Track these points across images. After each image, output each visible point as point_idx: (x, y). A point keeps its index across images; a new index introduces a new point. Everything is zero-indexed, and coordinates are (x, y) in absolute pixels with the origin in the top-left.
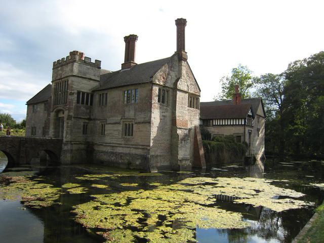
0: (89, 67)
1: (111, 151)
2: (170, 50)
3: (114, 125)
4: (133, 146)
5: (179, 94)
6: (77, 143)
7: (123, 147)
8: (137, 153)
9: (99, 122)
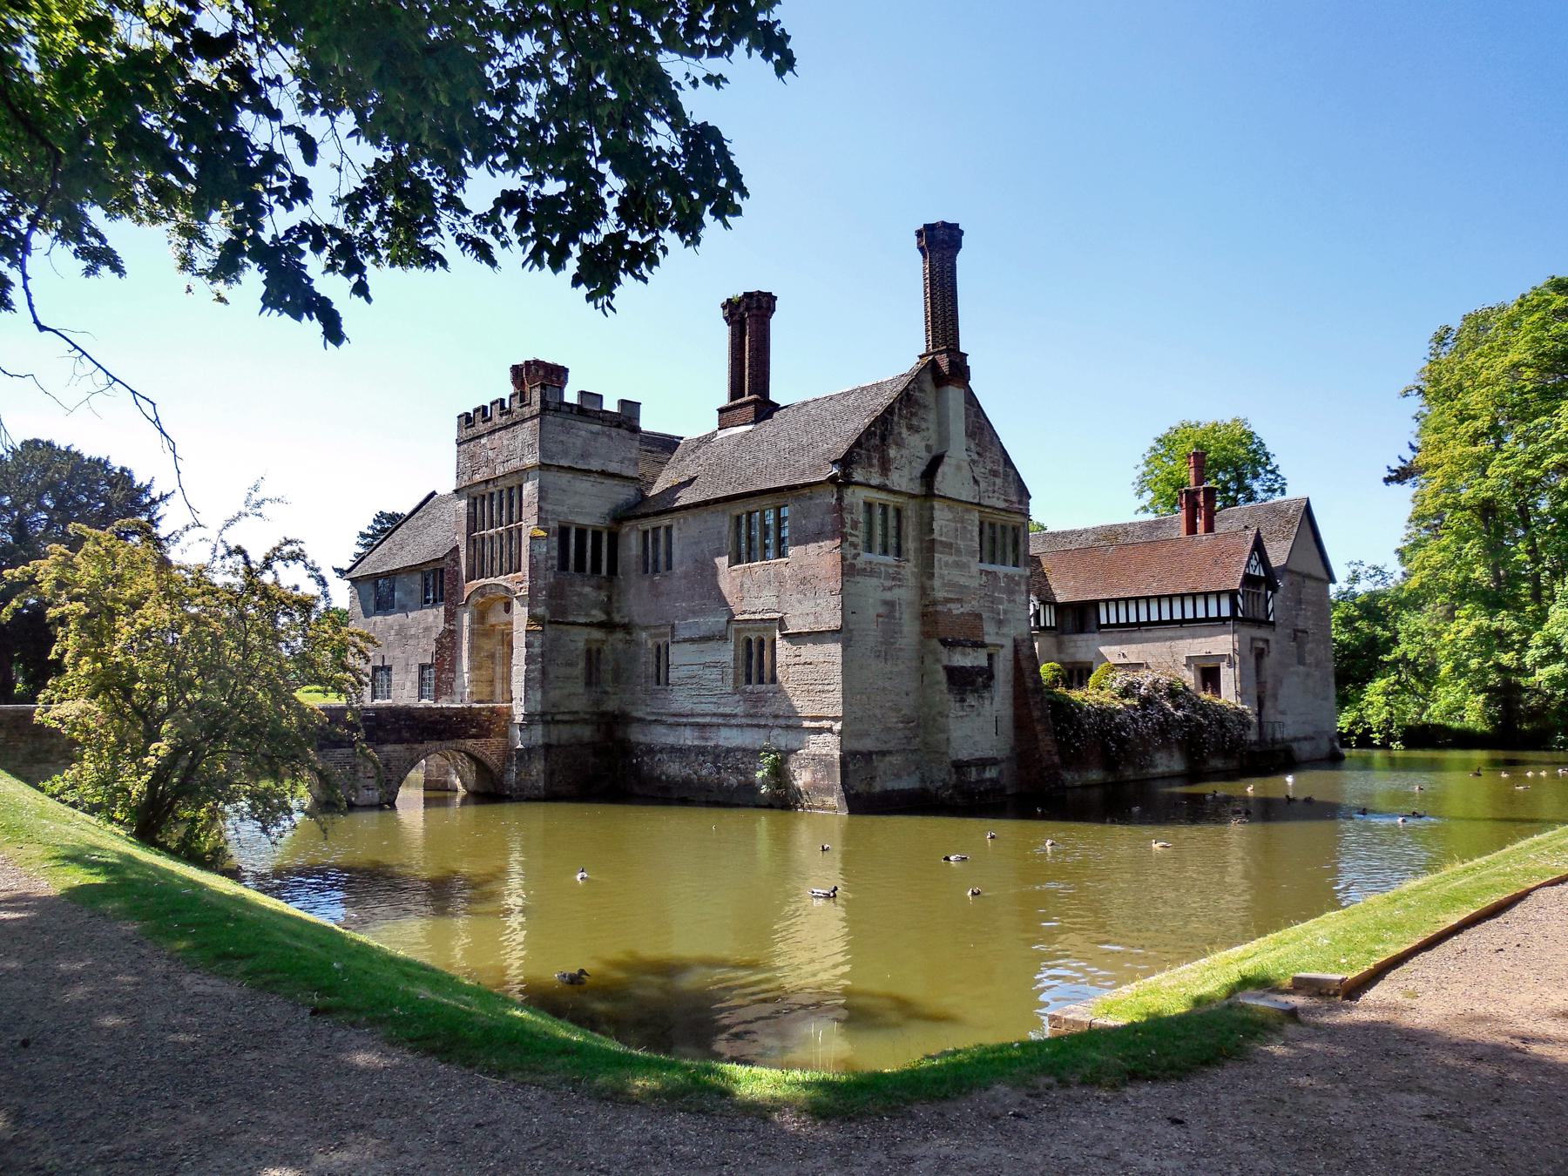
0: (596, 428)
2: (900, 350)
3: (703, 646)
4: (782, 722)
5: (942, 518)
6: (566, 717)
9: (644, 635)
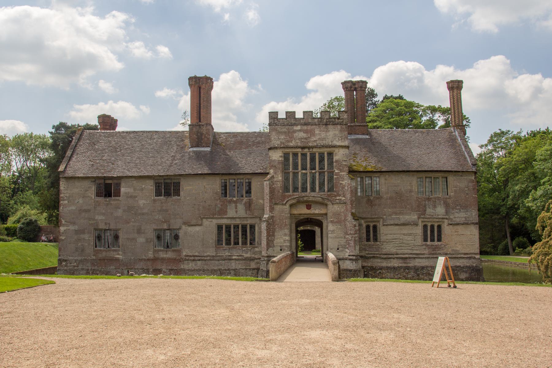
1: (400, 265)
3: (402, 227)
7: (428, 258)
8: (458, 264)
